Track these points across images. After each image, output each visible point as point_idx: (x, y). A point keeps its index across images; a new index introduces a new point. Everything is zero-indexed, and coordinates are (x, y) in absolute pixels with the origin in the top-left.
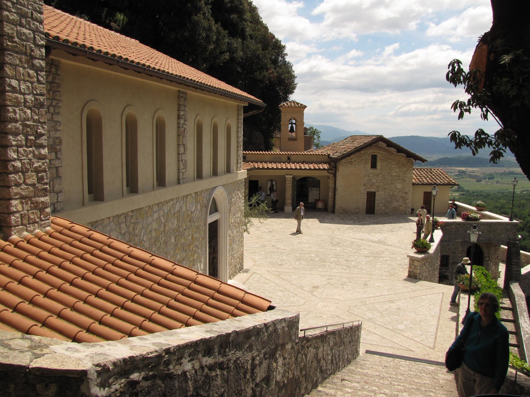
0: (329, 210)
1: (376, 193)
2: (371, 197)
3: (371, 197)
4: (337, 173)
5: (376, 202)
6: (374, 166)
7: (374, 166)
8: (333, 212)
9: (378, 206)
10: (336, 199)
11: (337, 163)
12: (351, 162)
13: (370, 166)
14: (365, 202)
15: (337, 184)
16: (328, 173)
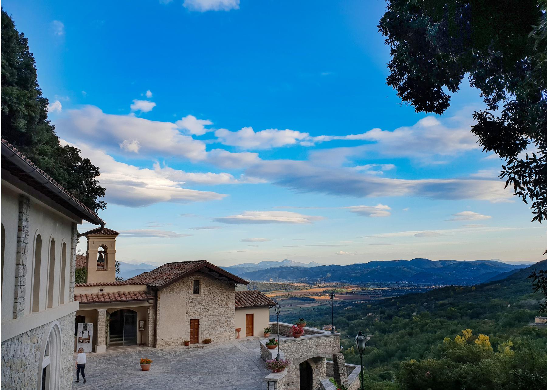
0: (150, 345)
1: (200, 321)
2: (195, 325)
3: (195, 325)
4: (158, 302)
5: (201, 330)
6: (197, 291)
7: (197, 291)
8: (154, 346)
9: (203, 334)
10: (158, 331)
11: (159, 293)
12: (172, 290)
13: (193, 292)
14: (189, 331)
15: (158, 314)
16: (148, 303)
